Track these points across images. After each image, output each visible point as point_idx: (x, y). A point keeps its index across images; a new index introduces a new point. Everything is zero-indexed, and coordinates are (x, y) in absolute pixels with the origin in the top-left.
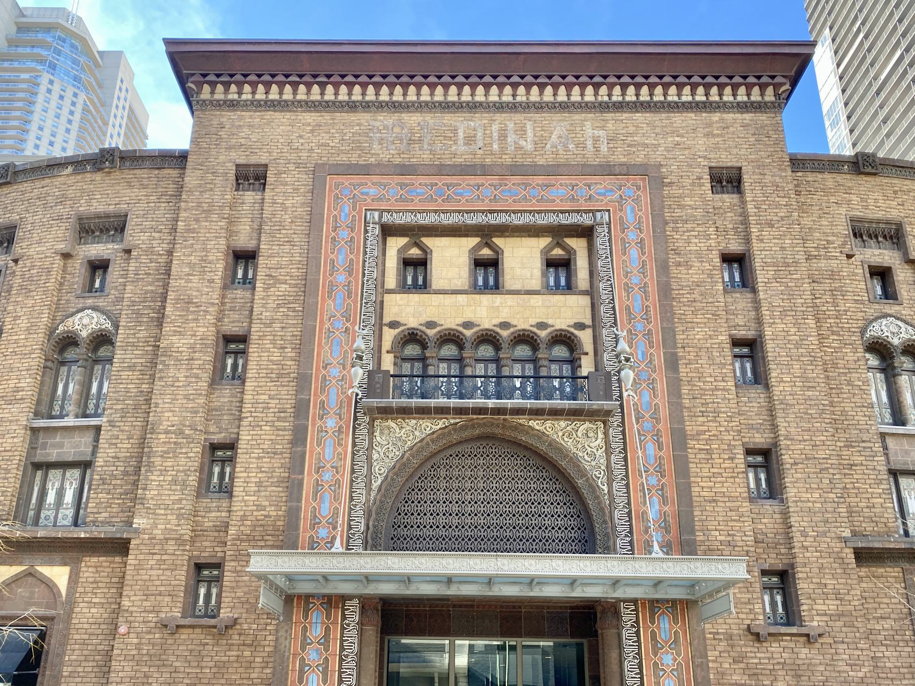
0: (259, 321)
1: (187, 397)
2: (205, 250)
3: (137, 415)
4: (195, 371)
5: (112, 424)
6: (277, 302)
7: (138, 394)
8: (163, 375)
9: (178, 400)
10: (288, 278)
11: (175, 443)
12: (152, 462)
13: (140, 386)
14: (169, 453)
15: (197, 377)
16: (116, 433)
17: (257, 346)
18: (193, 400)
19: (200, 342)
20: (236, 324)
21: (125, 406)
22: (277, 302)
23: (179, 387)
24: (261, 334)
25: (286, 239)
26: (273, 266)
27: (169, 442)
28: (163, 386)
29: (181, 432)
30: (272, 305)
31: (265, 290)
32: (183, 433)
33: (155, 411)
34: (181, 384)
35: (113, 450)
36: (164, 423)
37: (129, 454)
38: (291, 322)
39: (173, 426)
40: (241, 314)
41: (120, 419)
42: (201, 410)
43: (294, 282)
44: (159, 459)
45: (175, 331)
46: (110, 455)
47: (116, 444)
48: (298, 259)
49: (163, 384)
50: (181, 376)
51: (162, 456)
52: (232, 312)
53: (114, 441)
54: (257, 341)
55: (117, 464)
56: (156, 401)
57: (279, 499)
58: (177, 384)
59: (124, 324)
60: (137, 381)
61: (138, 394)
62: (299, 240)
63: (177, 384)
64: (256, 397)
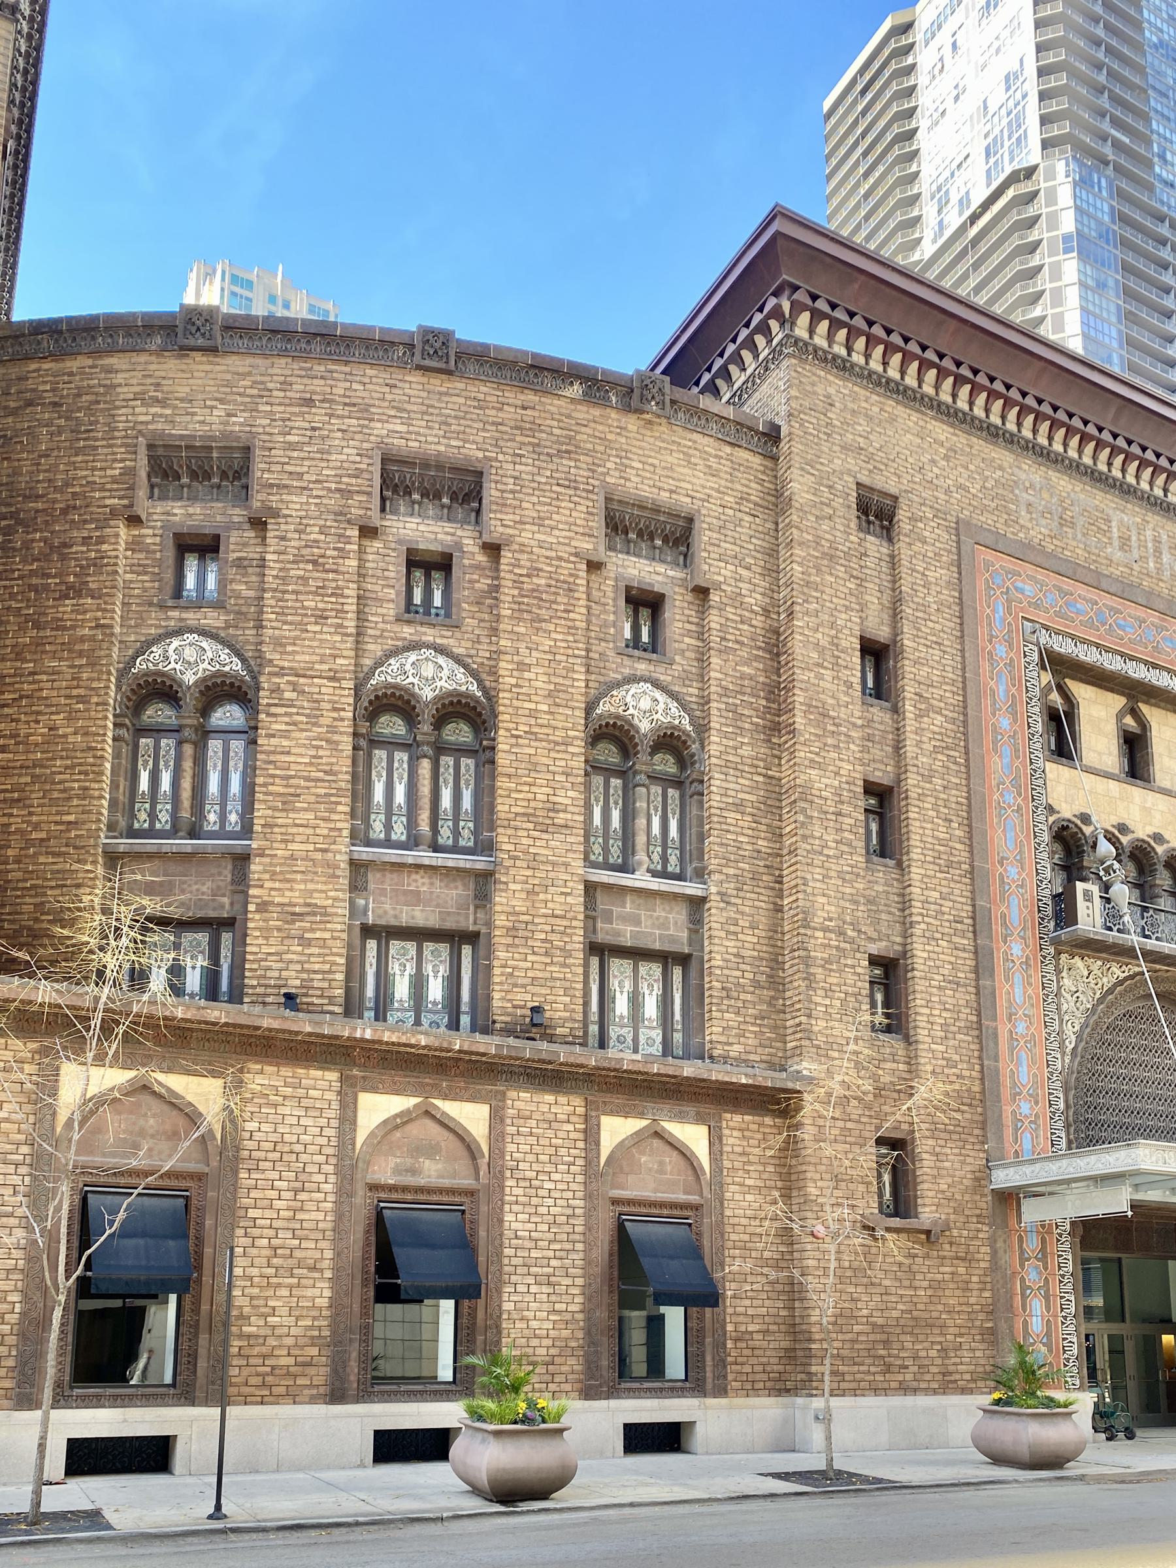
0: (915, 769)
1: (841, 875)
2: (833, 625)
3: (759, 890)
4: (846, 834)
5: (725, 898)
6: (933, 743)
7: (755, 855)
8: (808, 833)
9: (831, 878)
10: (942, 705)
11: (837, 948)
12: (812, 974)
13: (754, 841)
14: (831, 964)
15: (850, 845)
16: (733, 915)
17: (917, 810)
18: (850, 881)
19: (846, 786)
20: (878, 765)
21: (740, 872)
22: (933, 743)
23: (828, 856)
24: (920, 791)
25: (934, 639)
26: (922, 680)
27: (829, 946)
28: (808, 852)
29: (841, 933)
30: (928, 747)
31: (918, 717)
32: (845, 934)
33: (805, 891)
34: (831, 853)
35: (732, 944)
36: (819, 913)
37: (756, 954)
38: (954, 780)
39: (831, 920)
40: (882, 750)
41: (735, 892)
42: (862, 900)
43: (951, 715)
44: (820, 970)
45: (812, 761)
46: (730, 950)
47: (736, 933)
48: (950, 675)
49: (809, 847)
50: (830, 837)
51: (823, 966)
52: (870, 744)
53: (732, 928)
54: (917, 803)
55: (742, 966)
56: (803, 874)
57: (970, 1053)
58: (826, 851)
59: (718, 726)
60: (750, 832)
61: (755, 855)
62: (949, 643)
63: (826, 851)
64: (926, 892)
